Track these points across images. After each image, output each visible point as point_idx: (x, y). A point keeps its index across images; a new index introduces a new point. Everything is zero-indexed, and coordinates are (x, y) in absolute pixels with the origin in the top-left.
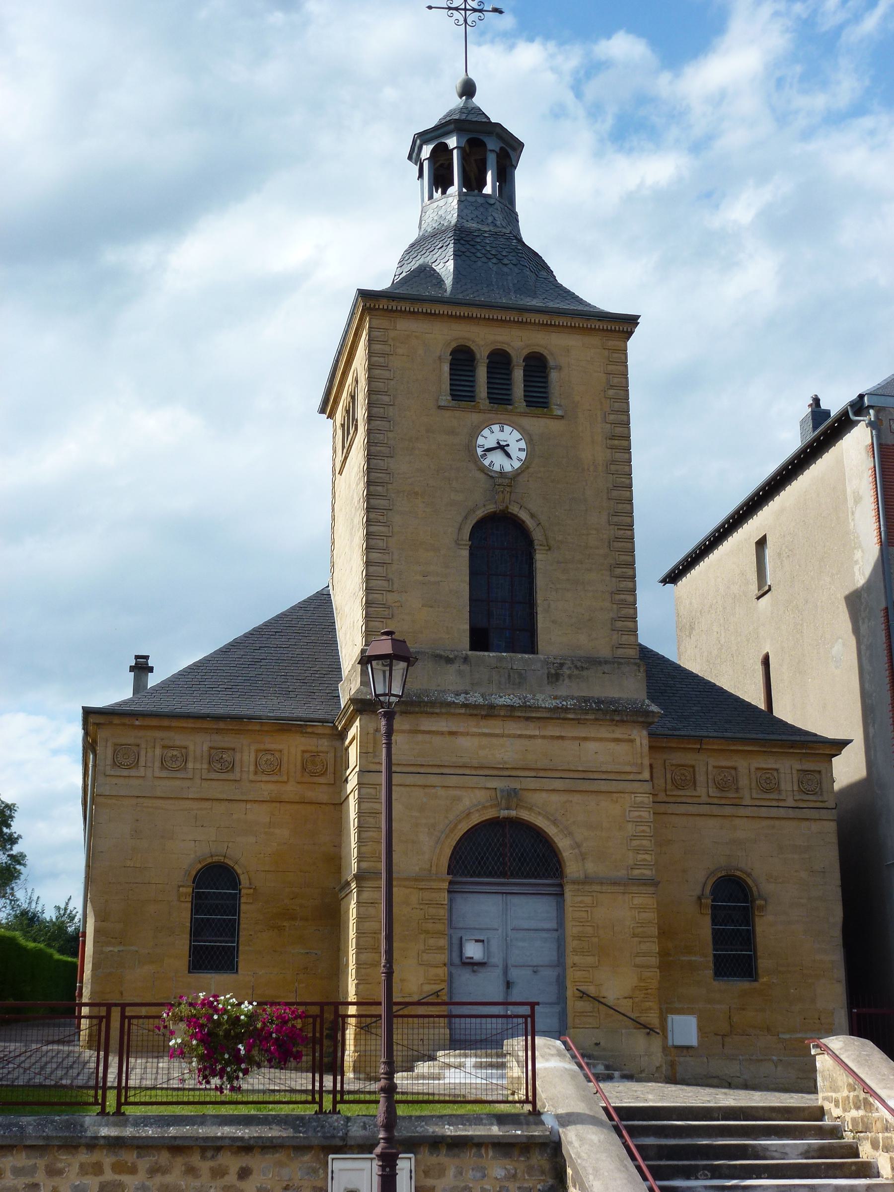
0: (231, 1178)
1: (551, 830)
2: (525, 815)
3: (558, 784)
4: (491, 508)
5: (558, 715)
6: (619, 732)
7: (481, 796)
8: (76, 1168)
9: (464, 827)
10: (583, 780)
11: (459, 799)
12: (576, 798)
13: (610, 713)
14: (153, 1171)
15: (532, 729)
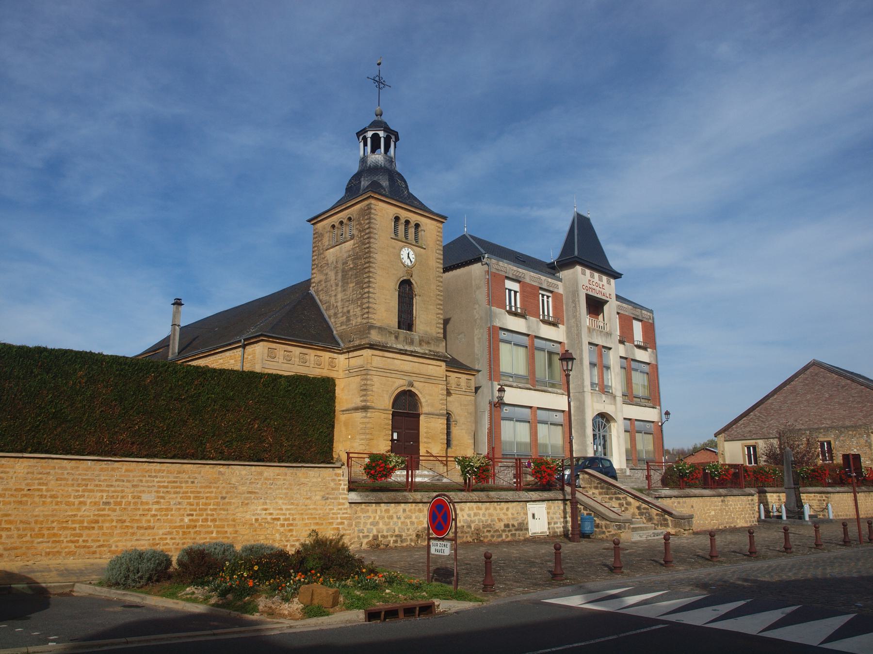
0: (505, 511)
1: (420, 395)
2: (412, 389)
3: (422, 380)
4: (405, 278)
5: (423, 356)
6: (439, 363)
7: (401, 382)
8: (467, 509)
9: (396, 392)
10: (429, 379)
11: (394, 382)
12: (426, 385)
13: (436, 357)
14: (487, 509)
15: (415, 359)
